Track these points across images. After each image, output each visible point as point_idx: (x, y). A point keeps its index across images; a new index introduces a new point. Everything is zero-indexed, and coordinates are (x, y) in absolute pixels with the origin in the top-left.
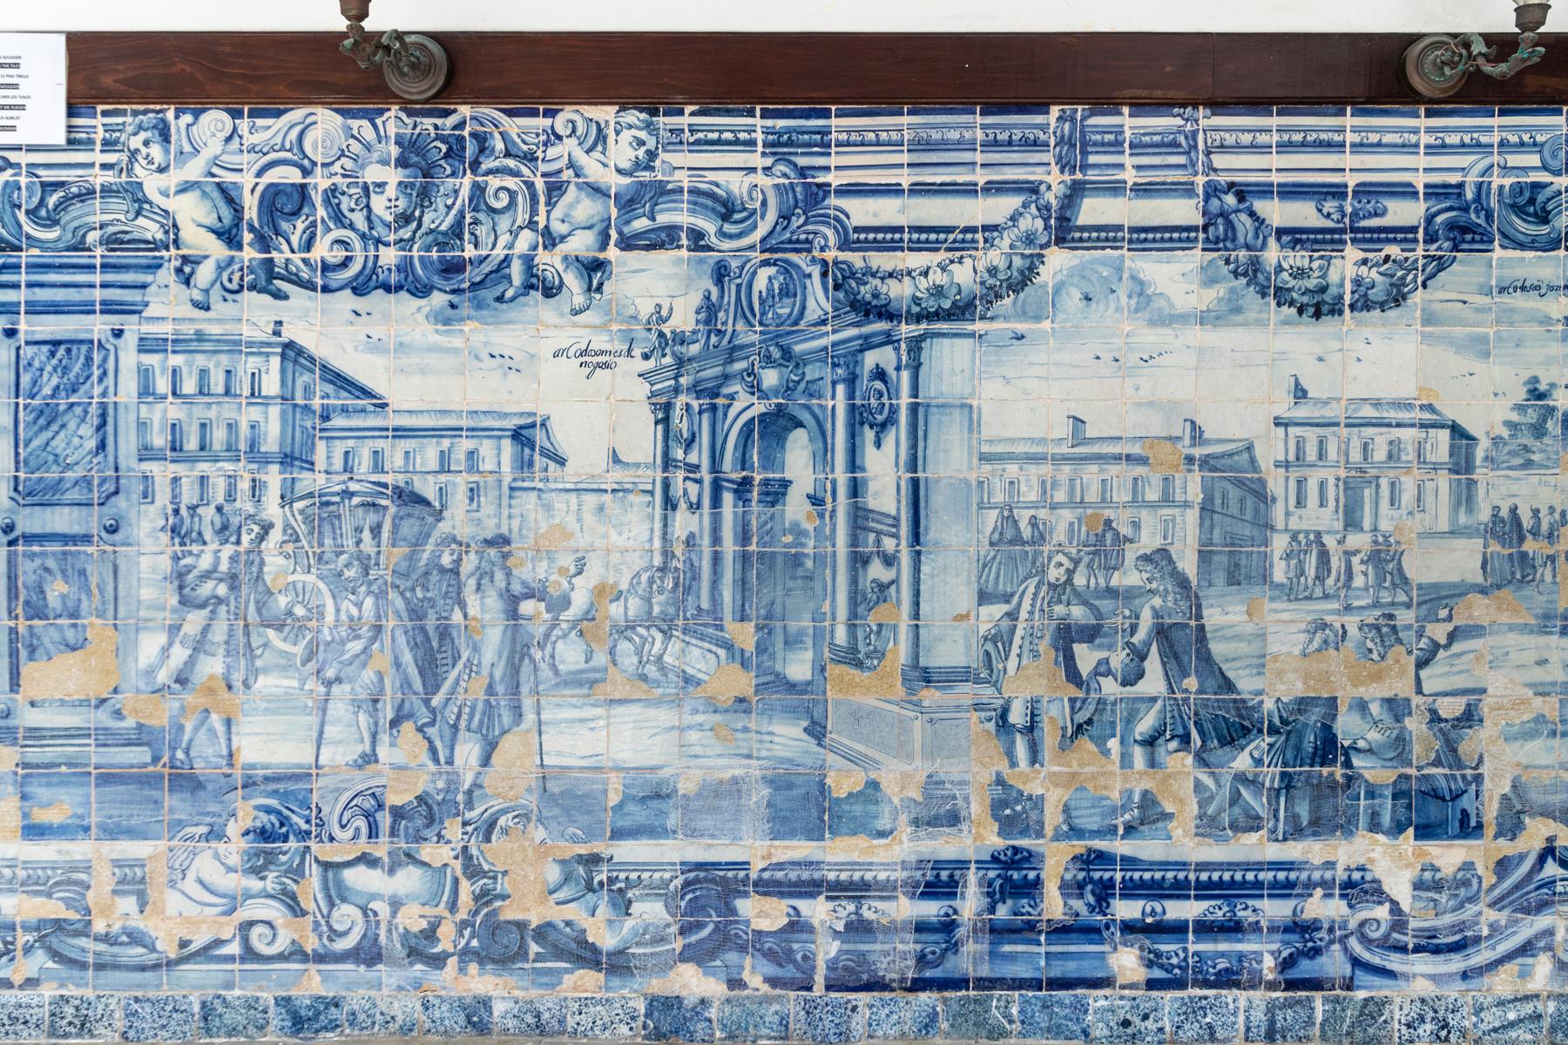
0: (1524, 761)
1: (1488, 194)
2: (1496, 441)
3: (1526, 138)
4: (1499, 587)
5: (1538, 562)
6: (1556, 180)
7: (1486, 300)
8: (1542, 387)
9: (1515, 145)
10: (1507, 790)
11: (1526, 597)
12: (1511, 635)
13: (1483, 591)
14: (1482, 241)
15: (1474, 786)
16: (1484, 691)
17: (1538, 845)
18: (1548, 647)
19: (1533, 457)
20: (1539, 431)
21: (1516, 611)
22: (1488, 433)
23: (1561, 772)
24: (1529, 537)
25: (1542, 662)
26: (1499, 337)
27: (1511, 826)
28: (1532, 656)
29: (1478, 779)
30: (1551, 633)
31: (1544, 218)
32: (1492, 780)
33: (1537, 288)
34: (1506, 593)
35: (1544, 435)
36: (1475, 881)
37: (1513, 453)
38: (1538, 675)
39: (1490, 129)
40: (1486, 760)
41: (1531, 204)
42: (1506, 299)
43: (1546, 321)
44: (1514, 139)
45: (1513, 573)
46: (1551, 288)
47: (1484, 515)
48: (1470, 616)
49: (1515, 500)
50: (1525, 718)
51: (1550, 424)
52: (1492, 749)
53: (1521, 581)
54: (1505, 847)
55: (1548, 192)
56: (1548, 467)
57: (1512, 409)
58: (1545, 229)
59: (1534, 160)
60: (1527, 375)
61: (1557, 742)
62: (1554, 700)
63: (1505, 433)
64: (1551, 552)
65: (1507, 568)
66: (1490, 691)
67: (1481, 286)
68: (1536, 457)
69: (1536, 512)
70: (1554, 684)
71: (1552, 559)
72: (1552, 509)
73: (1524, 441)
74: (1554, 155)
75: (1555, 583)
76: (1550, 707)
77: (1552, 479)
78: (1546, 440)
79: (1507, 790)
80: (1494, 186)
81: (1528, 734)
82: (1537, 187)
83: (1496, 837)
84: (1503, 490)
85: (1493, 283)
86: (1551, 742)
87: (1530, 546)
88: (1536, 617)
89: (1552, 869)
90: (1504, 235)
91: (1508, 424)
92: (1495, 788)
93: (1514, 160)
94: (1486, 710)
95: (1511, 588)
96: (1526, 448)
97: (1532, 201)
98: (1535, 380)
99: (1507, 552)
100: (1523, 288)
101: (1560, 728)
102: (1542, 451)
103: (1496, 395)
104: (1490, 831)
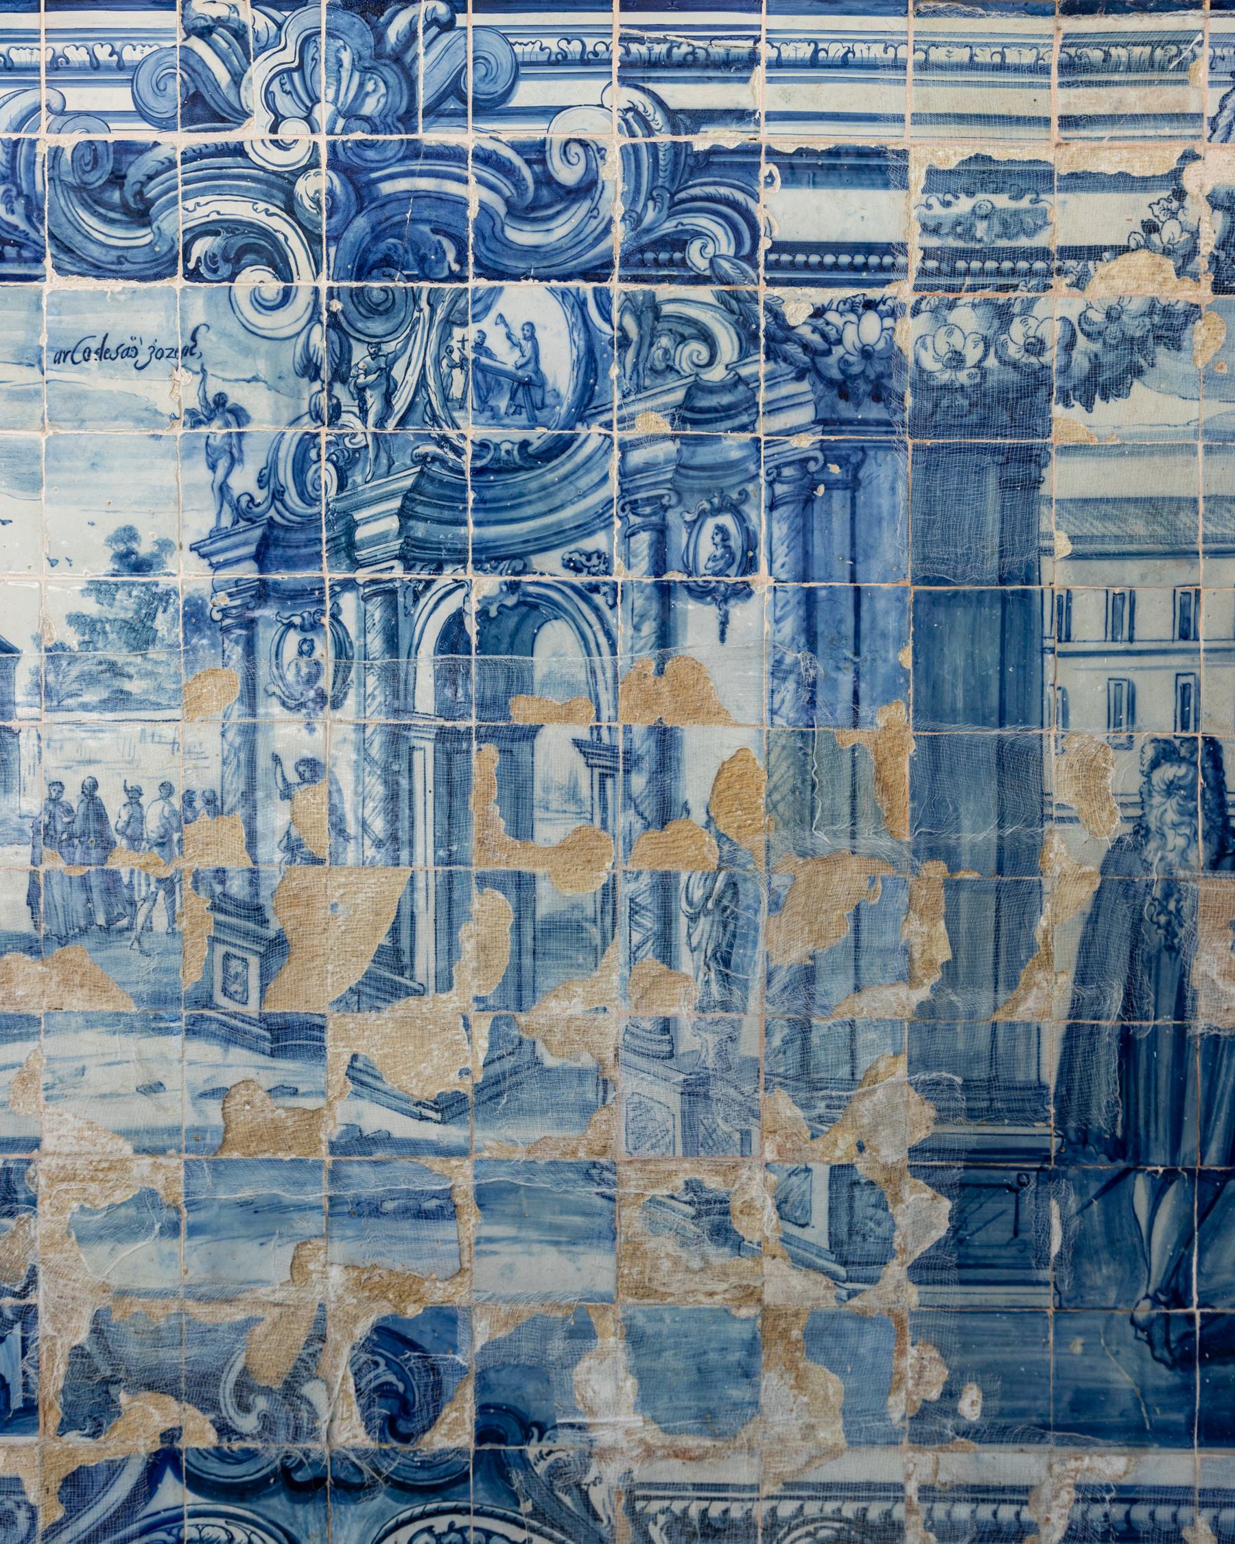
0: (116, 1282)
1: (31, 164)
2: (55, 653)
3: (103, 54)
4: (63, 941)
5: (141, 891)
6: (164, 137)
7: (32, 375)
8: (144, 549)
9: (81, 69)
10: (82, 1336)
11: (116, 961)
12: (89, 1035)
13: (32, 947)
14: (20, 260)
15: (17, 1330)
16: (36, 1144)
17: (145, 1445)
18: (164, 1058)
19: (128, 686)
20: (139, 634)
21: (99, 988)
22: (38, 639)
23: (192, 1306)
24: (122, 842)
25: (155, 1088)
26: (54, 453)
27: (92, 1408)
28: (134, 1076)
29: (27, 1315)
30: (168, 1031)
31: (140, 215)
32: (54, 1318)
33: (129, 352)
34: (76, 952)
35: (150, 642)
36: (22, 1516)
37: (89, 679)
38: (144, 1113)
39: (29, 37)
40: (41, 1278)
41: (113, 182)
42: (66, 374)
43: (148, 417)
44: (78, 56)
45: (90, 914)
46: (158, 353)
47: (32, 802)
48: (9, 997)
49: (93, 771)
50: (119, 1196)
51: (161, 622)
52: (54, 1257)
53: (107, 929)
54: (82, 1449)
55: (149, 162)
56: (157, 706)
57: (85, 592)
58: (143, 237)
59: (120, 98)
60: (113, 524)
61: (181, 1245)
62: (174, 1163)
63: (72, 639)
64: (166, 873)
65: (78, 898)
66: (48, 1143)
67: (22, 350)
68: (134, 687)
69: (134, 795)
70: (174, 1131)
71: (169, 885)
72: (167, 789)
73: (110, 655)
74: (159, 89)
75: (172, 933)
76: (165, 1175)
77: (168, 731)
78: (154, 653)
79: (82, 1336)
80: (42, 149)
81: (121, 1229)
82: (126, 149)
83: (63, 1429)
84: (70, 750)
85: (44, 341)
86: (168, 1245)
87: (122, 862)
88: (138, 999)
89: (172, 1493)
90: (64, 248)
91: (76, 620)
92: (62, 1334)
93: (80, 98)
94: (42, 1181)
95: (88, 943)
96: (114, 669)
97: (117, 179)
98: (129, 534)
99: (77, 872)
100: (102, 353)
101: (186, 1218)
102: (149, 674)
103: (53, 563)
104: (52, 1417)
